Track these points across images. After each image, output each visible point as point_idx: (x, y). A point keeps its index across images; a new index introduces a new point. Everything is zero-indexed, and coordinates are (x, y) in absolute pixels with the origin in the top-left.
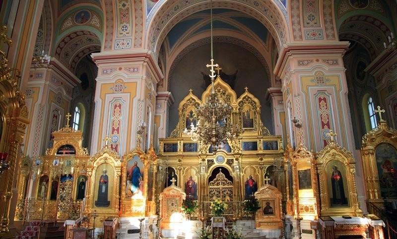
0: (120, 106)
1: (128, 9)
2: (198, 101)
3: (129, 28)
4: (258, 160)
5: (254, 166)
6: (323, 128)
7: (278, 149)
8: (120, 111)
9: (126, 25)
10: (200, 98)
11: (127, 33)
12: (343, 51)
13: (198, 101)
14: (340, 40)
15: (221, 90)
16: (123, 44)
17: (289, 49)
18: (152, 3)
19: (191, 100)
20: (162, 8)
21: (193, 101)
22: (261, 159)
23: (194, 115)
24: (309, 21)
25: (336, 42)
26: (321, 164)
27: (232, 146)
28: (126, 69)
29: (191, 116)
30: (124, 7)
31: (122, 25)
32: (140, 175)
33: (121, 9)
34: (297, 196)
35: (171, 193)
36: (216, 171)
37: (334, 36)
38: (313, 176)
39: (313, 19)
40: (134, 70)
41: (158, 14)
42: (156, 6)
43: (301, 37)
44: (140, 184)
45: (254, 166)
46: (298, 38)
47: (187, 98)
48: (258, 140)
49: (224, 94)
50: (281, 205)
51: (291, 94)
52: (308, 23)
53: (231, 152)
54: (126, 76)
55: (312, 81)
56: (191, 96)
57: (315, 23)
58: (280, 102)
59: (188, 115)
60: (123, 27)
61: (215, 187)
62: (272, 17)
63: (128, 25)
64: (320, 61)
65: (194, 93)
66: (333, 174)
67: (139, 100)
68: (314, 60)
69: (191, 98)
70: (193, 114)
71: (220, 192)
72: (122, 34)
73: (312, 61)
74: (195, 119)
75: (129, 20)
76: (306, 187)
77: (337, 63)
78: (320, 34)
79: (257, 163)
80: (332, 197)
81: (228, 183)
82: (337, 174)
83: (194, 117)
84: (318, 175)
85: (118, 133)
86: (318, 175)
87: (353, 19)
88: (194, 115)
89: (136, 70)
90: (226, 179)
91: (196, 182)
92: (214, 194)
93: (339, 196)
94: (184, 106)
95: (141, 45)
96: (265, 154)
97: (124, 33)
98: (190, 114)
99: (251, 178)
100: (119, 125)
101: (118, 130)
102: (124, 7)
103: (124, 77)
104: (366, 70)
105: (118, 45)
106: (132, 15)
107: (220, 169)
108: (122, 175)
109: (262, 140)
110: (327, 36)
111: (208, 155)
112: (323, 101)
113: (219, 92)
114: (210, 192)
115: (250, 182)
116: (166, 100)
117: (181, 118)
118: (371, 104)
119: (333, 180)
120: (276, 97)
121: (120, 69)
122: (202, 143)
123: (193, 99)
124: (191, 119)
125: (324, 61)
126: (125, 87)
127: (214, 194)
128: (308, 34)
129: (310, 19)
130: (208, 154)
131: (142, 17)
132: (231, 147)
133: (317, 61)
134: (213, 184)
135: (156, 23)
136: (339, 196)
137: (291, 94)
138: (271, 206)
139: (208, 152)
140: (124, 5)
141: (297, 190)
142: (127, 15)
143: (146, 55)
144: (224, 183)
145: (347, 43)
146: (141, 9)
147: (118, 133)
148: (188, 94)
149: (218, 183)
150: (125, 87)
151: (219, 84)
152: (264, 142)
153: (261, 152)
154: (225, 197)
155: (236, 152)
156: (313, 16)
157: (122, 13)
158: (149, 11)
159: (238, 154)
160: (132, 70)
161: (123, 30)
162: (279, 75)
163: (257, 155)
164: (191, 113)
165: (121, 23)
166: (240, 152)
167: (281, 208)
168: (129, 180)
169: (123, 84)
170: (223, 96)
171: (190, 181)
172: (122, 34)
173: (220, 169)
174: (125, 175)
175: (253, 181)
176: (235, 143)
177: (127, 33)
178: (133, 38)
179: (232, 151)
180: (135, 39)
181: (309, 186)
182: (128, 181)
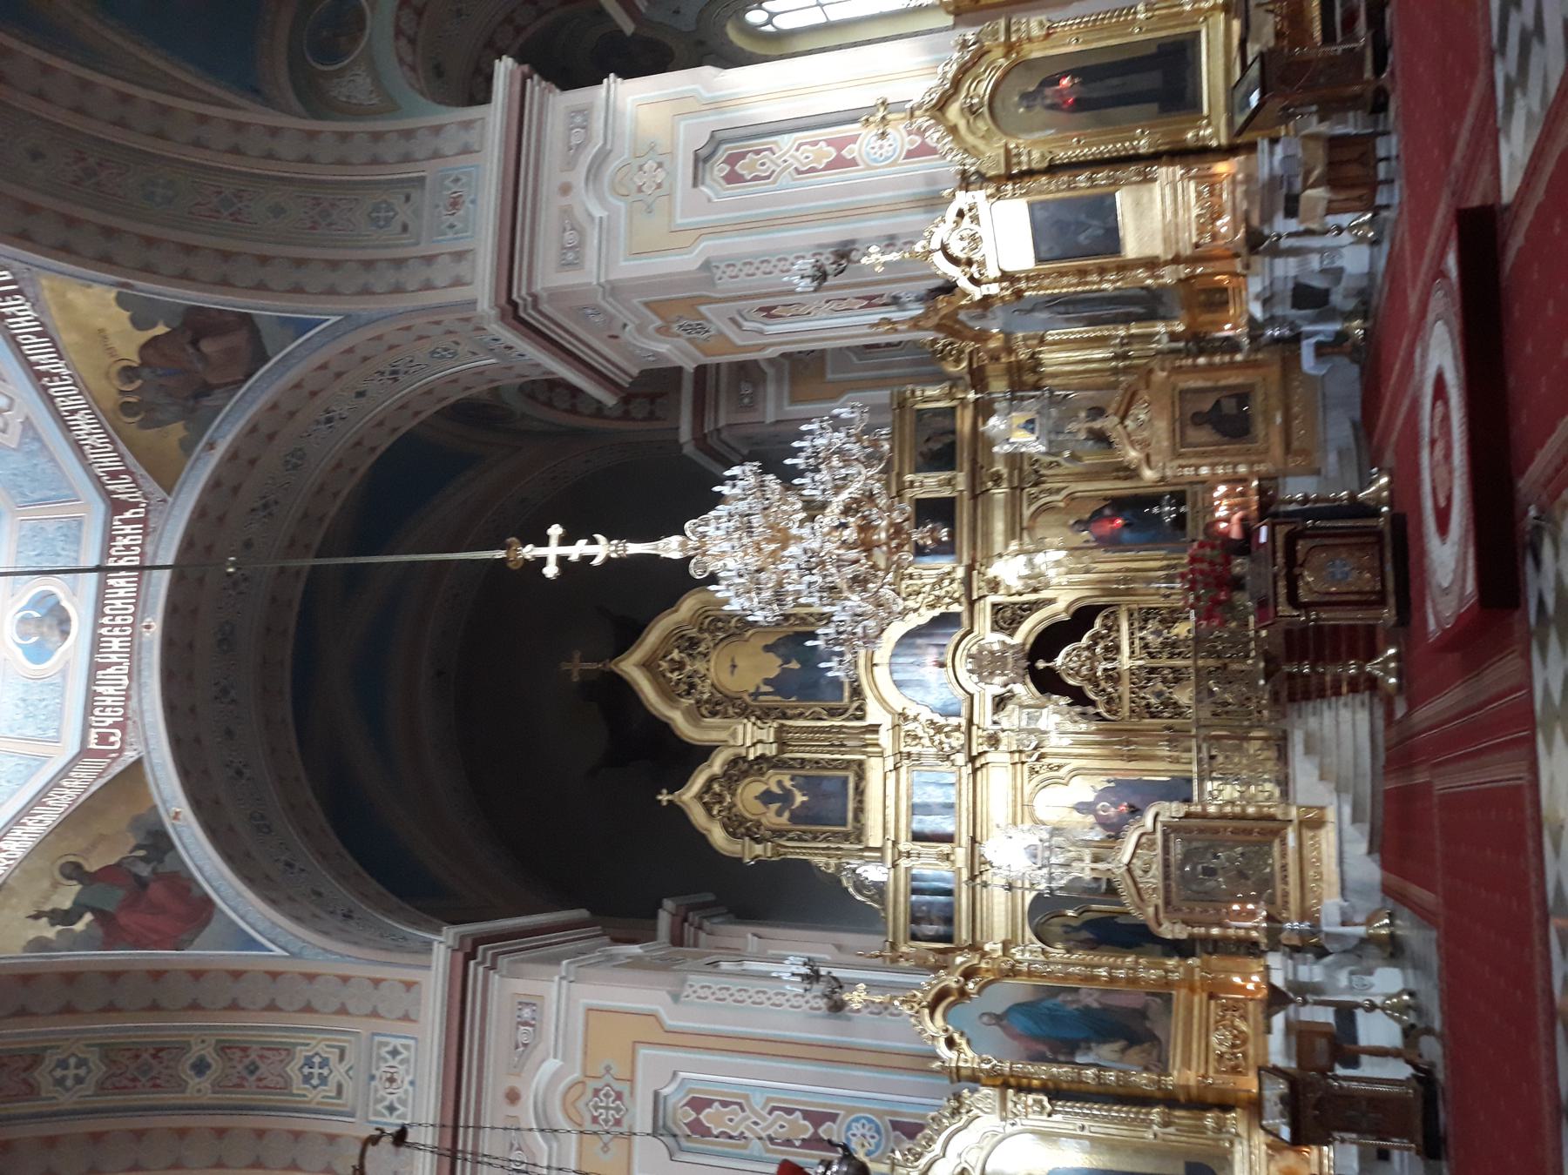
0: (698, 1104)
1: (224, 1048)
2: (717, 765)
3: (320, 1046)
4: (1000, 493)
5: (1027, 513)
6: (853, 163)
7: (953, 409)
8: (725, 1104)
9: (299, 1061)
10: (704, 753)
11: (342, 1058)
12: (536, 86)
13: (717, 765)
14: (485, 98)
15: (675, 655)
16: (391, 1080)
17: (503, 301)
18: (214, 927)
19: (707, 798)
20: (249, 880)
21: (716, 787)
22: (997, 479)
23: (780, 783)
24: (396, 226)
25: (494, 116)
26: (1008, 151)
27: (933, 606)
28: (517, 1069)
29: (786, 797)
30: (209, 1066)
31: (297, 1086)
32: (1049, 1003)
33: (217, 1086)
34: (1151, 264)
35: (1154, 879)
36: (1048, 683)
37: (467, 125)
38: (1052, 189)
39: (390, 208)
40: (528, 1014)
41: (273, 902)
42: (235, 910)
43: (459, 256)
44: (1095, 1005)
45: (1027, 513)
46: (463, 269)
47: (698, 816)
48: (908, 494)
49: (693, 643)
50: (1202, 360)
51: (703, 309)
52: (405, 228)
53: (958, 615)
54: (552, 1065)
55: (649, 210)
56: (688, 795)
57: (408, 198)
58: (746, 401)
59: (779, 813)
60: (307, 1079)
61: (1125, 688)
62: (361, 394)
63: (301, 1053)
64: (567, 177)
65: (680, 782)
66: (1053, 107)
67: (676, 998)
68: (564, 201)
69: (699, 797)
70: (776, 790)
71: (1152, 670)
72: (340, 1087)
73: (567, 212)
74: (800, 780)
75: (275, 1049)
76: (1111, 219)
77: (585, 112)
78: (457, 180)
79: (1013, 495)
80: (1154, 107)
81: (1110, 629)
82: (1049, 91)
83: (788, 783)
84: (1052, 169)
85: (833, 1117)
86: (1052, 169)
87: (409, 59)
88: (780, 783)
89: (527, 1013)
90: (1085, 640)
91: (1101, 783)
92: (1159, 694)
93: (1150, 80)
94: (733, 835)
95: (409, 985)
96: (974, 461)
97: (338, 1073)
98: (775, 806)
99: (1082, 524)
100: (790, 1111)
101: (817, 1119)
102: (209, 1066)
103: (556, 1076)
104: (629, 27)
105: (391, 1109)
106: (252, 1025)
107: (1041, 664)
108: (1043, 1089)
109: (908, 477)
110: (466, 150)
111: (970, 722)
112: (737, 168)
113: (679, 666)
114: (1153, 716)
115: (1106, 528)
116: (700, 928)
117: (795, 850)
118: (772, 15)
119: (1081, 105)
120: (722, 423)
121: (513, 1097)
122: (914, 750)
123: (708, 787)
124: (800, 798)
125: (571, 164)
126: (608, 1069)
127: (1159, 694)
128: (452, 226)
129: (388, 220)
130: (963, 721)
131: (274, 975)
132: (936, 612)
133: (566, 189)
134: (1110, 701)
135: (314, 916)
136: (1150, 80)
137: (703, 309)
138: (1207, 406)
139: (954, 721)
140: (201, 1067)
141: (1125, 267)
142: (253, 1056)
143: (460, 956)
144: (1107, 649)
145: (504, 68)
146: (237, 975)
147: (833, 1117)
148: (677, 813)
149: (1109, 678)
150: (608, 1069)
151: (648, 666)
152: (917, 470)
153: (962, 480)
154: (1174, 645)
155: (957, 589)
156: (377, 209)
157: (235, 1081)
158: (252, 944)
159: (967, 582)
160: (524, 1034)
161: (324, 1080)
162: (625, 381)
163: (974, 497)
164: (767, 797)
165: (286, 1086)
166: (960, 573)
167: (1217, 359)
168: (1072, 1053)
169: (592, 1084)
170: (702, 649)
171: (1097, 816)
172: (340, 1087)
173: (1041, 664)
174: (1042, 1071)
175: (1097, 515)
176: (919, 593)
177: (342, 1058)
178: (363, 1027)
179: (955, 608)
180: (375, 1014)
181: (1104, 208)
182: (1079, 1059)
